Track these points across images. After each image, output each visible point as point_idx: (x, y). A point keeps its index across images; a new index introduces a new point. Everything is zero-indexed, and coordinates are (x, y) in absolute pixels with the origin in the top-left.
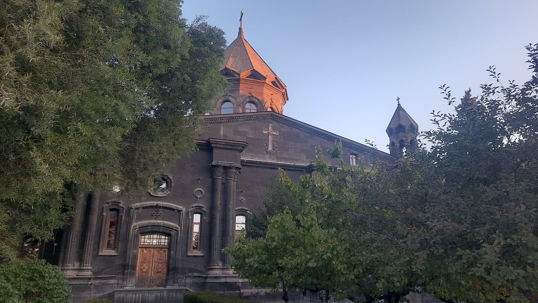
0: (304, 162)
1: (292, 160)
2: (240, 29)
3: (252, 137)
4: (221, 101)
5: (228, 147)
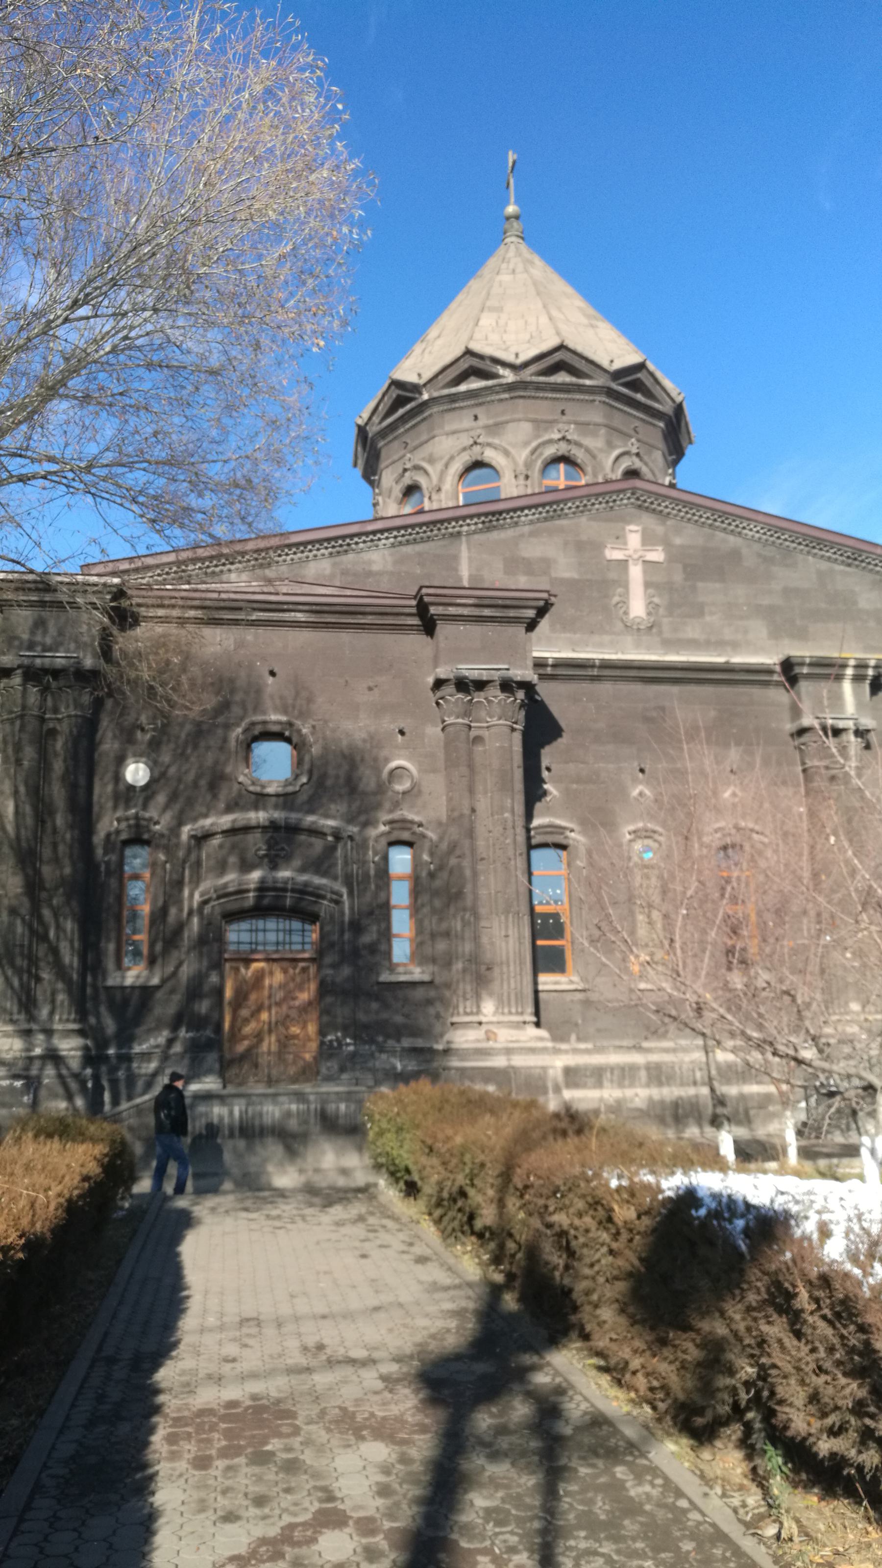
1: (720, 645)
3: (567, 575)
4: (457, 466)
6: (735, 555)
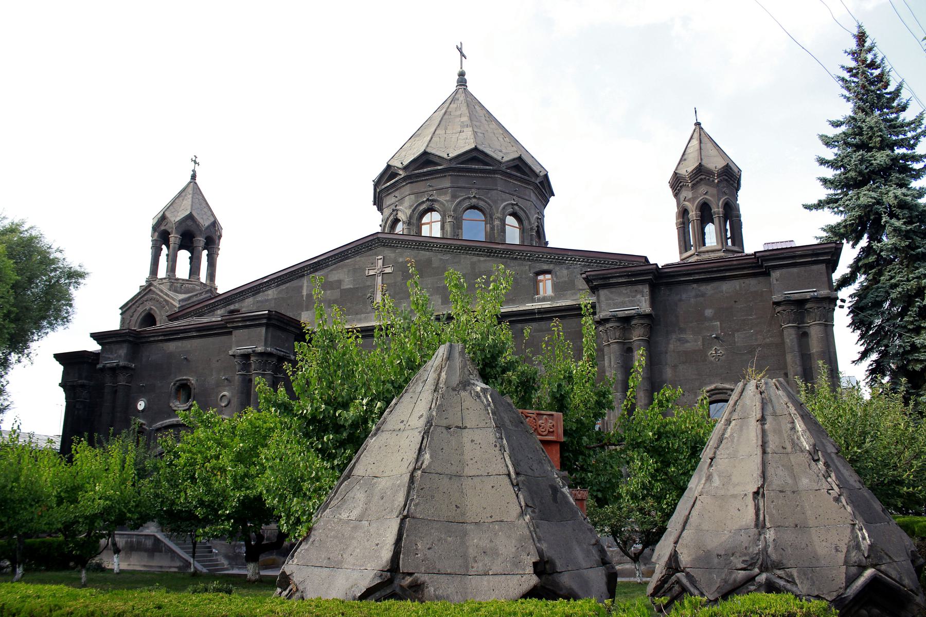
2: (462, 74)
3: (348, 287)
5: (248, 323)
6: (429, 261)
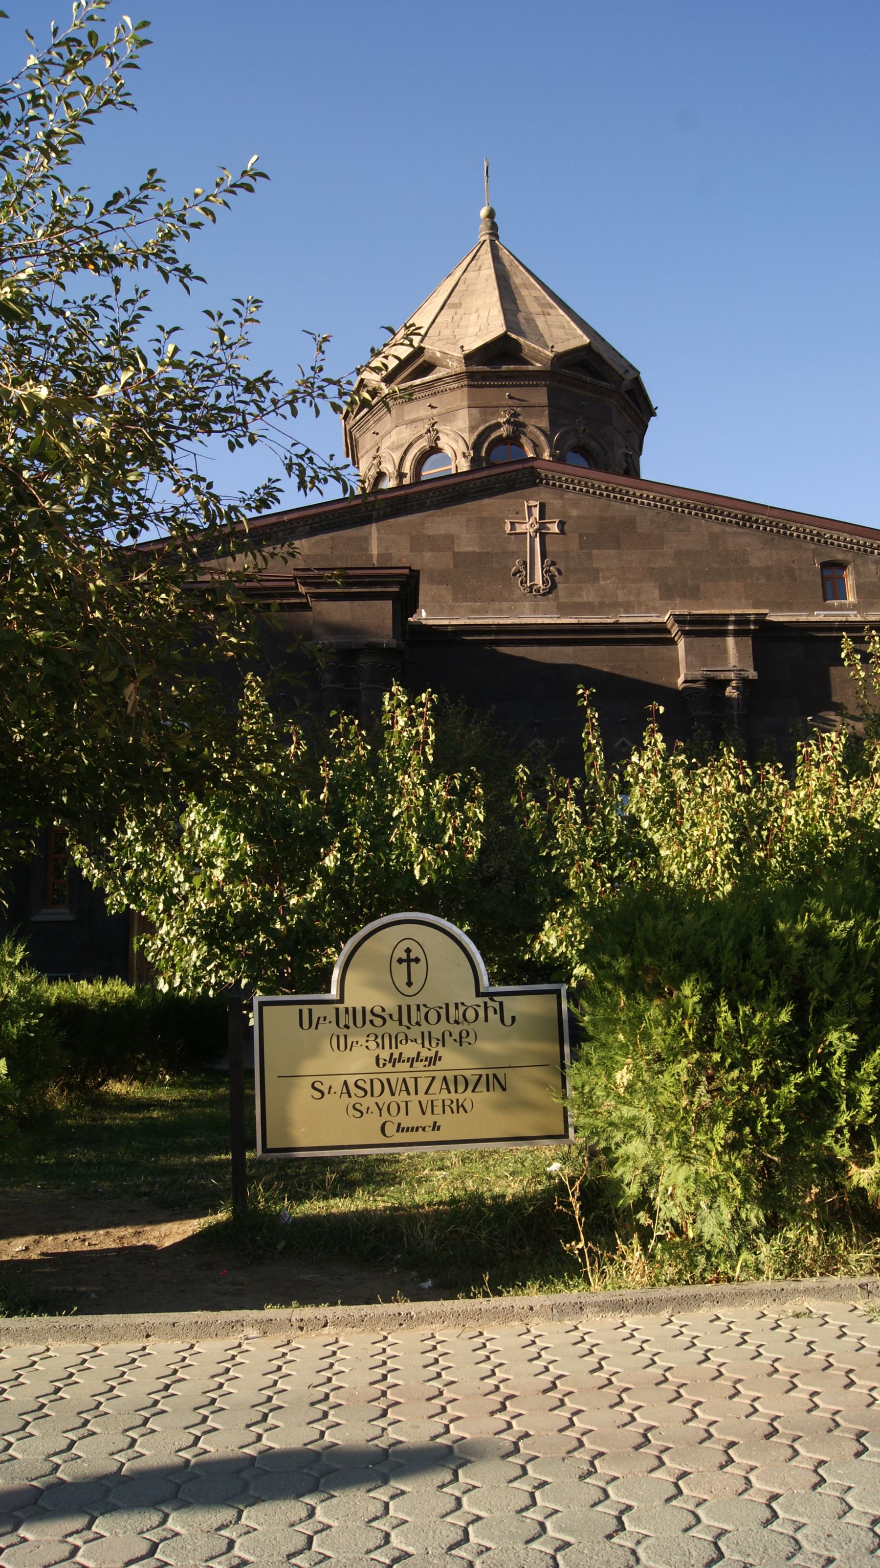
0: (654, 609)
1: (614, 606)
